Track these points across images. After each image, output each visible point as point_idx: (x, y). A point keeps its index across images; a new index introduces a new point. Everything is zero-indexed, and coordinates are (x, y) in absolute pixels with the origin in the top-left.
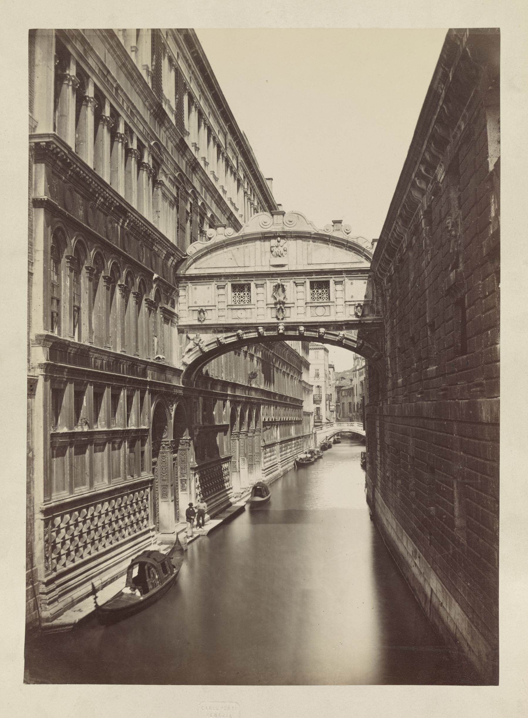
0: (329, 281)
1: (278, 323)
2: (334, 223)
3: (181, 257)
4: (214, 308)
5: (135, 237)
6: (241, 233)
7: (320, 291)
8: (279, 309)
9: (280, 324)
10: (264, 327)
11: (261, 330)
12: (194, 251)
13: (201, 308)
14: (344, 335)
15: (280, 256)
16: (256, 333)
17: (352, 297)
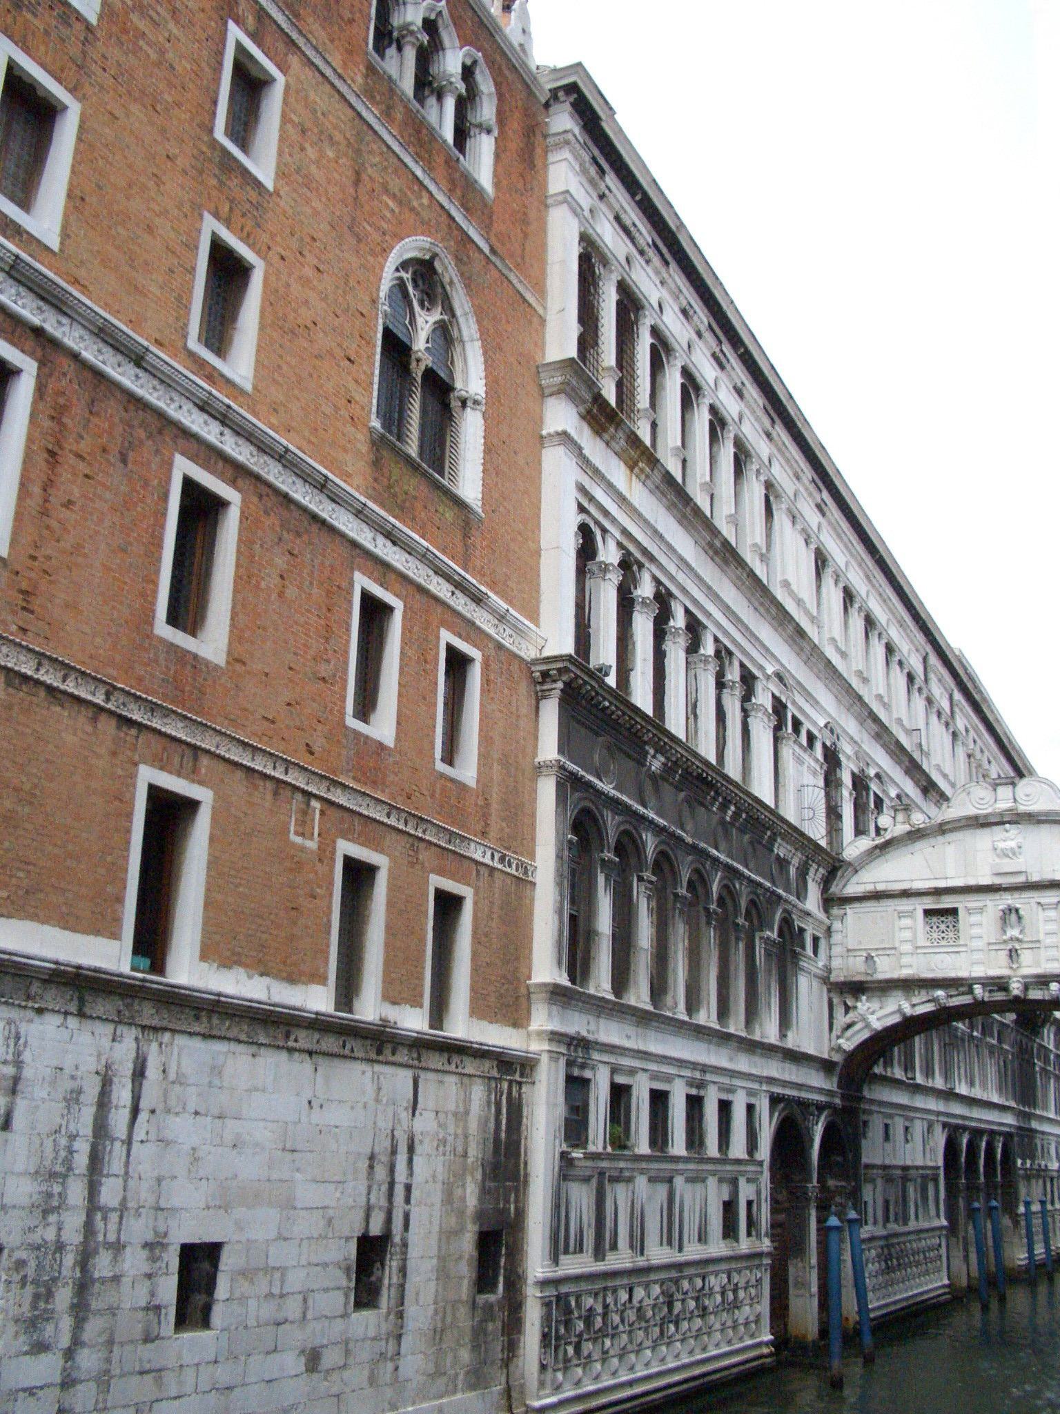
1: (1009, 978)
4: (892, 952)
5: (738, 829)
11: (978, 989)
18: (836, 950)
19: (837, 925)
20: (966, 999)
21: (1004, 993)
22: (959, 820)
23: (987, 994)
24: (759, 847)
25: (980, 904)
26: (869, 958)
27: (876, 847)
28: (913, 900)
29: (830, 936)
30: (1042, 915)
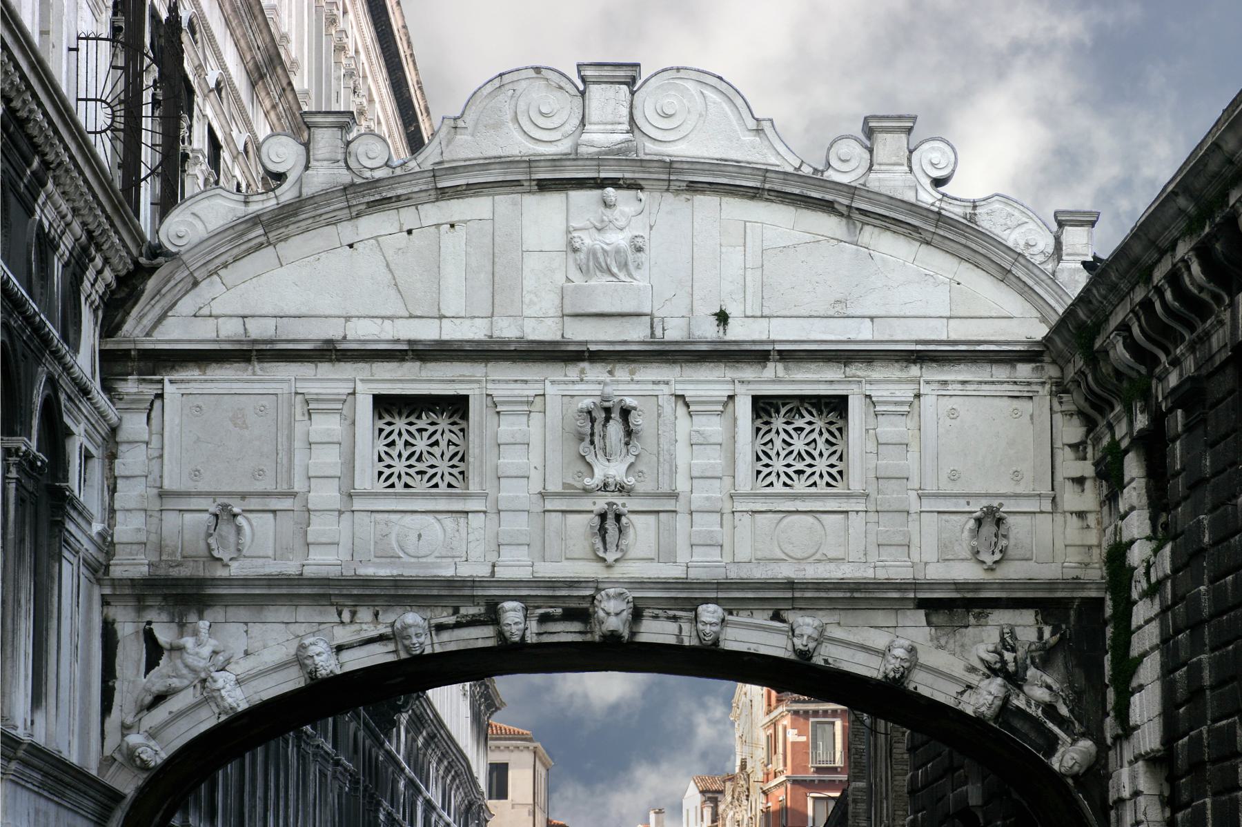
0: (843, 400)
1: (597, 585)
2: (870, 132)
3: (136, 263)
4: (286, 503)
6: (429, 156)
7: (799, 444)
8: (603, 516)
9: (612, 591)
10: (527, 610)
11: (512, 613)
12: (200, 232)
13: (220, 500)
14: (912, 650)
15: (613, 275)
16: (489, 631)
17: (954, 477)
18: (128, 494)
19: (134, 425)
20: (480, 637)
21: (577, 626)
22: (487, 164)
23: (533, 626)
24: (12, 200)
25: (530, 391)
26: (224, 515)
27: (255, 220)
28: (348, 370)
29: (112, 457)
30: (683, 423)
